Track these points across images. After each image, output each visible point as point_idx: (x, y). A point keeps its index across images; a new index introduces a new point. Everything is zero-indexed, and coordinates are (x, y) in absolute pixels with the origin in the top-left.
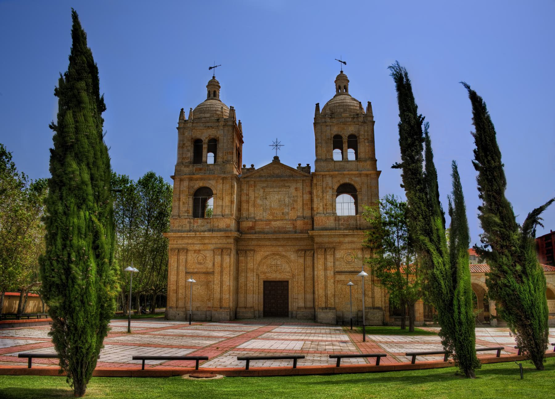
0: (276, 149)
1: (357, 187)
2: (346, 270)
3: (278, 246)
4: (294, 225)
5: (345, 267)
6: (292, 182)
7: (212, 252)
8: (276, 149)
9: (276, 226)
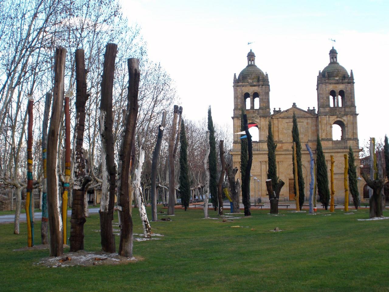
1: (345, 123)
2: (339, 172)
7: (260, 163)
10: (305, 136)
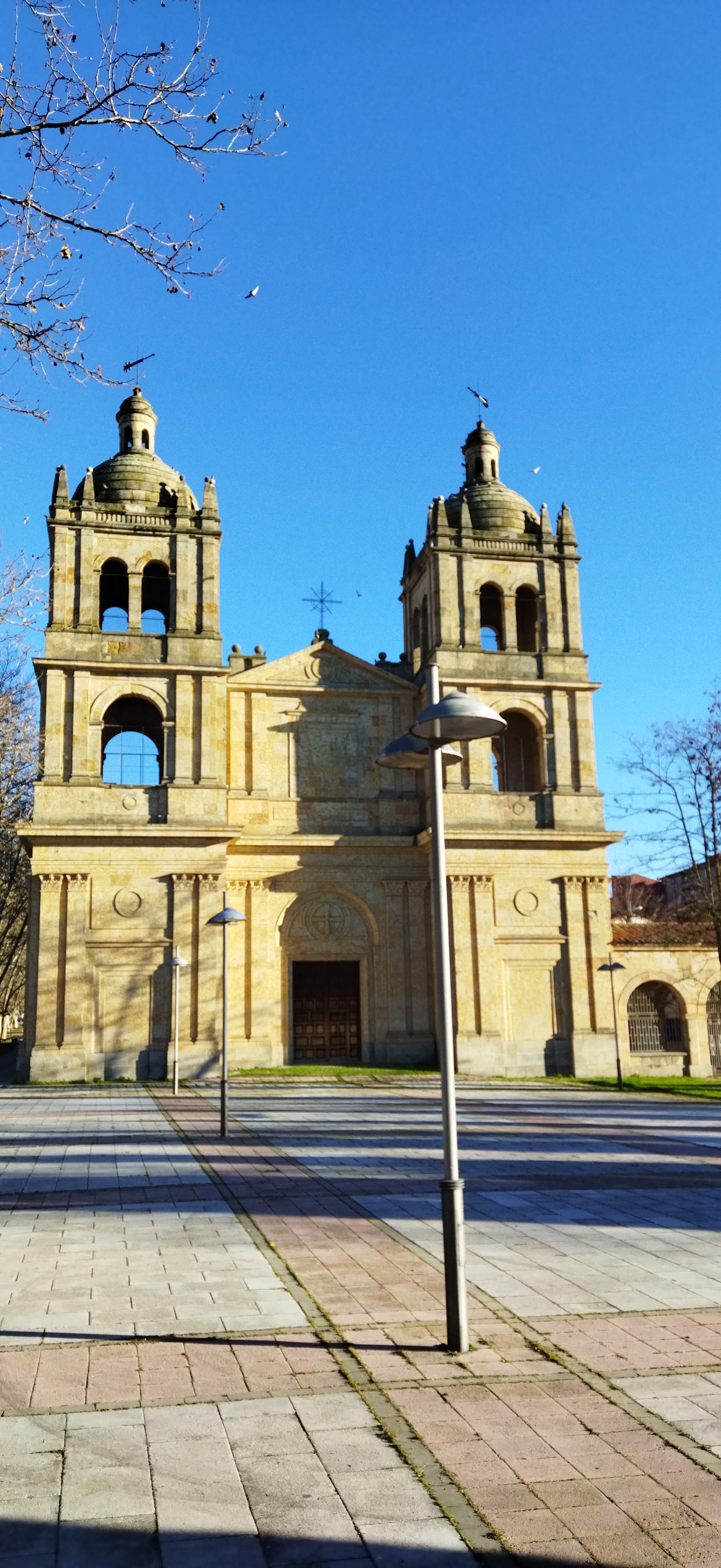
0: (322, 611)
2: (523, 932)
3: (335, 867)
4: (371, 812)
5: (521, 924)
6: (365, 700)
8: (322, 611)
9: (326, 813)
10: (364, 774)
